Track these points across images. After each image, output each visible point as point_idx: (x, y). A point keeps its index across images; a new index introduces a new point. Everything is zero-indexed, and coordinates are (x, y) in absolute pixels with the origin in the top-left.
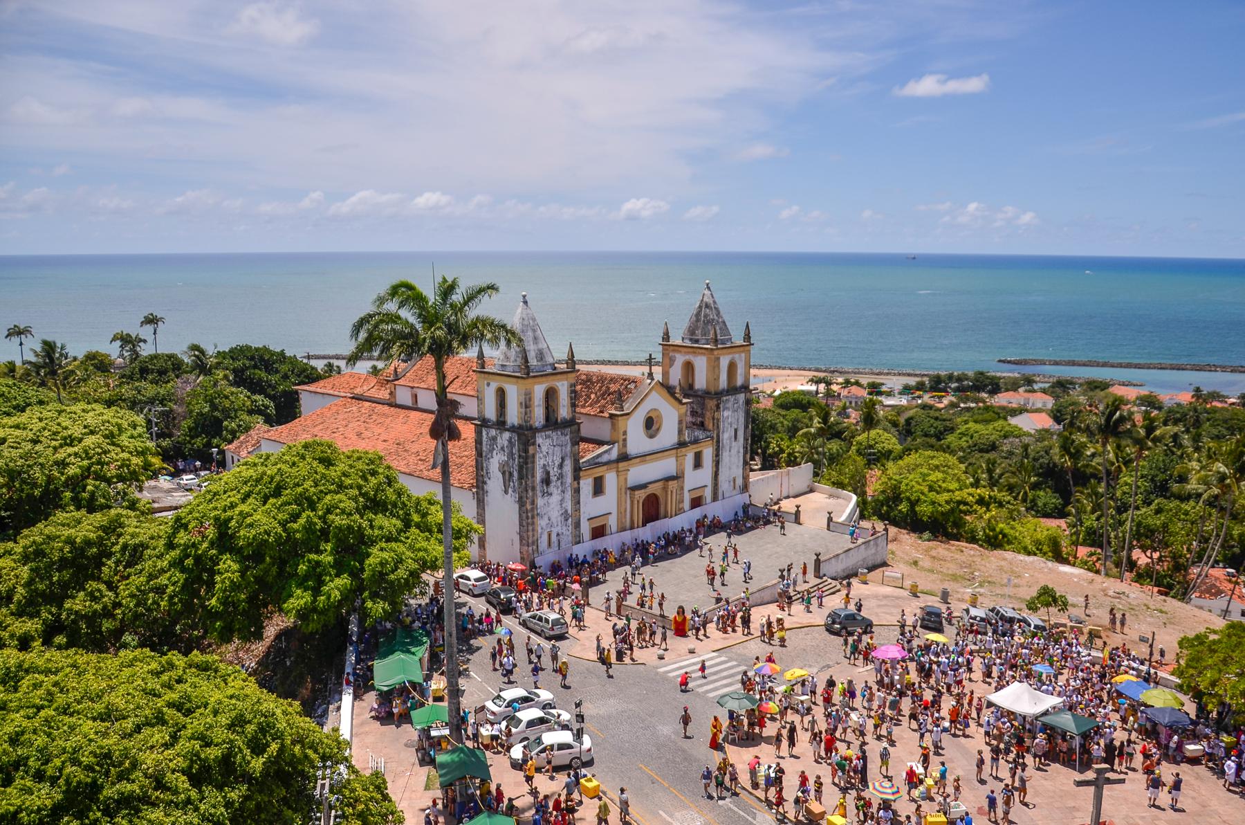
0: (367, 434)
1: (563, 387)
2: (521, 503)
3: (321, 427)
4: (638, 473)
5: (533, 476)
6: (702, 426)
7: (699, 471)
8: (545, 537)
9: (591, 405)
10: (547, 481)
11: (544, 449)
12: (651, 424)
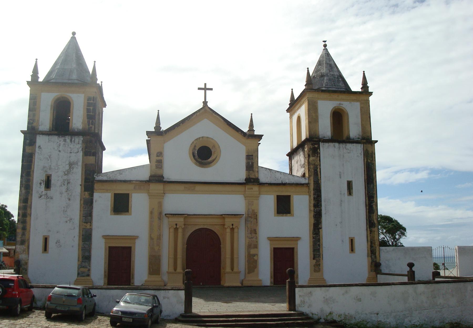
4: (177, 202)
10: (48, 184)
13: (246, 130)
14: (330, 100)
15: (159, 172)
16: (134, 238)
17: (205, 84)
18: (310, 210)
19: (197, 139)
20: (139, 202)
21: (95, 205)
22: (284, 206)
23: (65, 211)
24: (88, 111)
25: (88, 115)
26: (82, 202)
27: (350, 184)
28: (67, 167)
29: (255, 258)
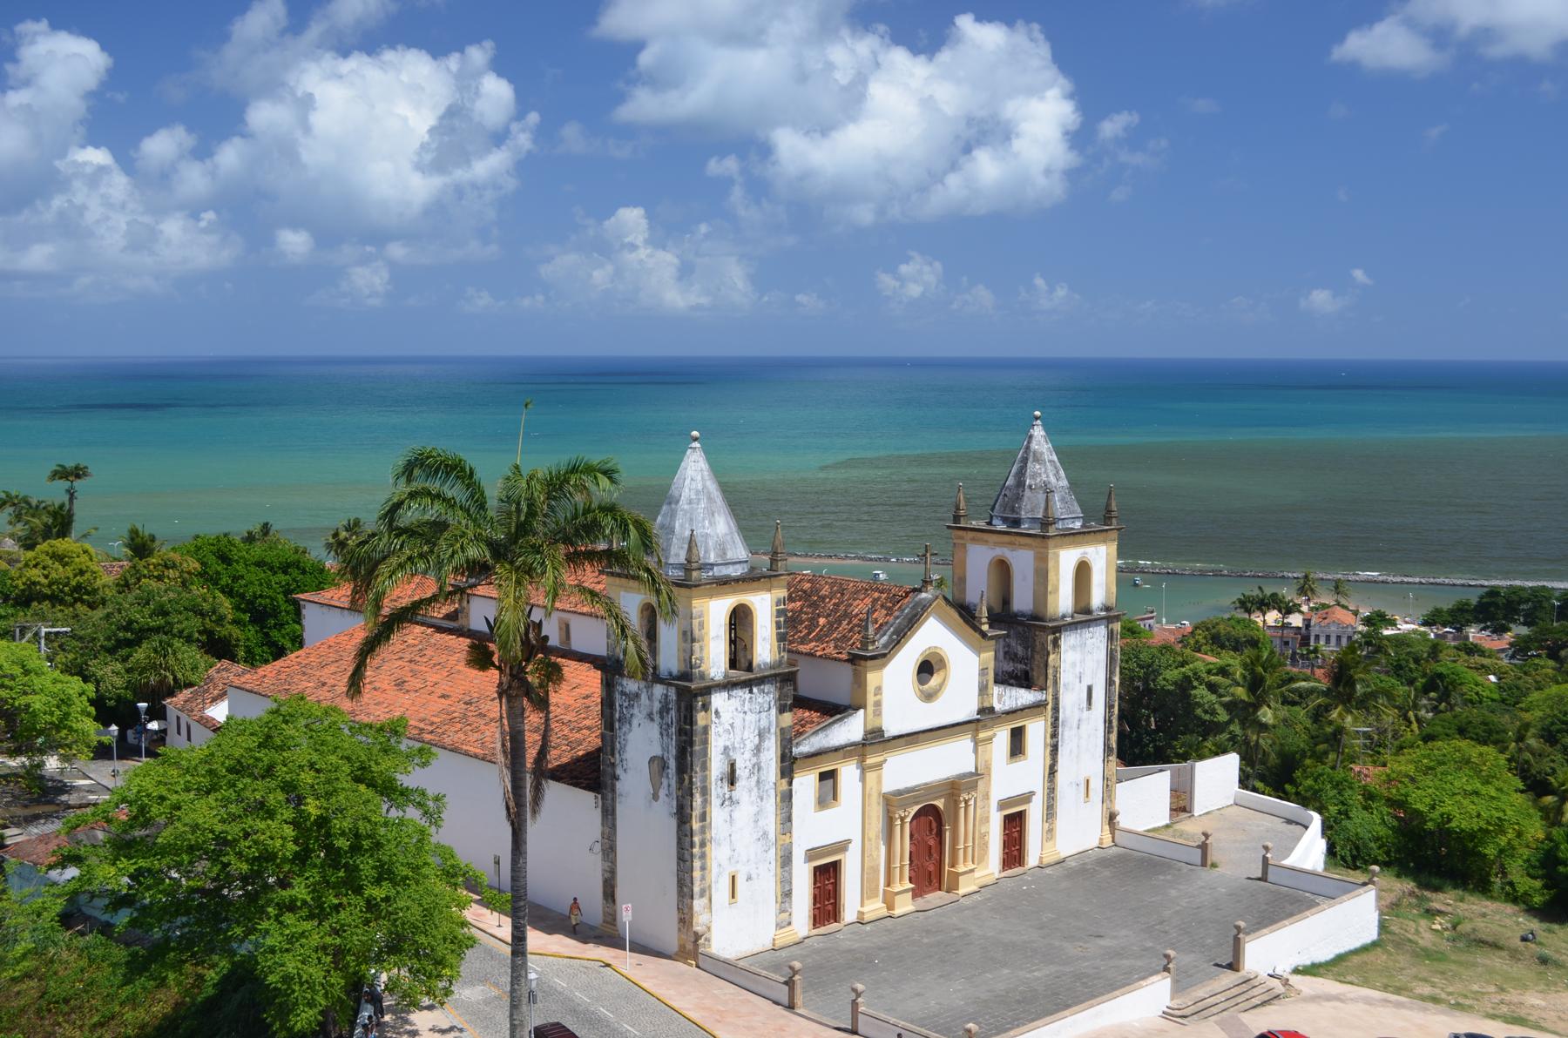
0: (415, 683)
1: (764, 605)
2: (683, 816)
3: (333, 668)
5: (705, 767)
6: (1024, 680)
7: (1020, 765)
8: (727, 882)
9: (819, 639)
11: (726, 717)
23: (756, 821)
27: (1090, 689)
28: (757, 740)
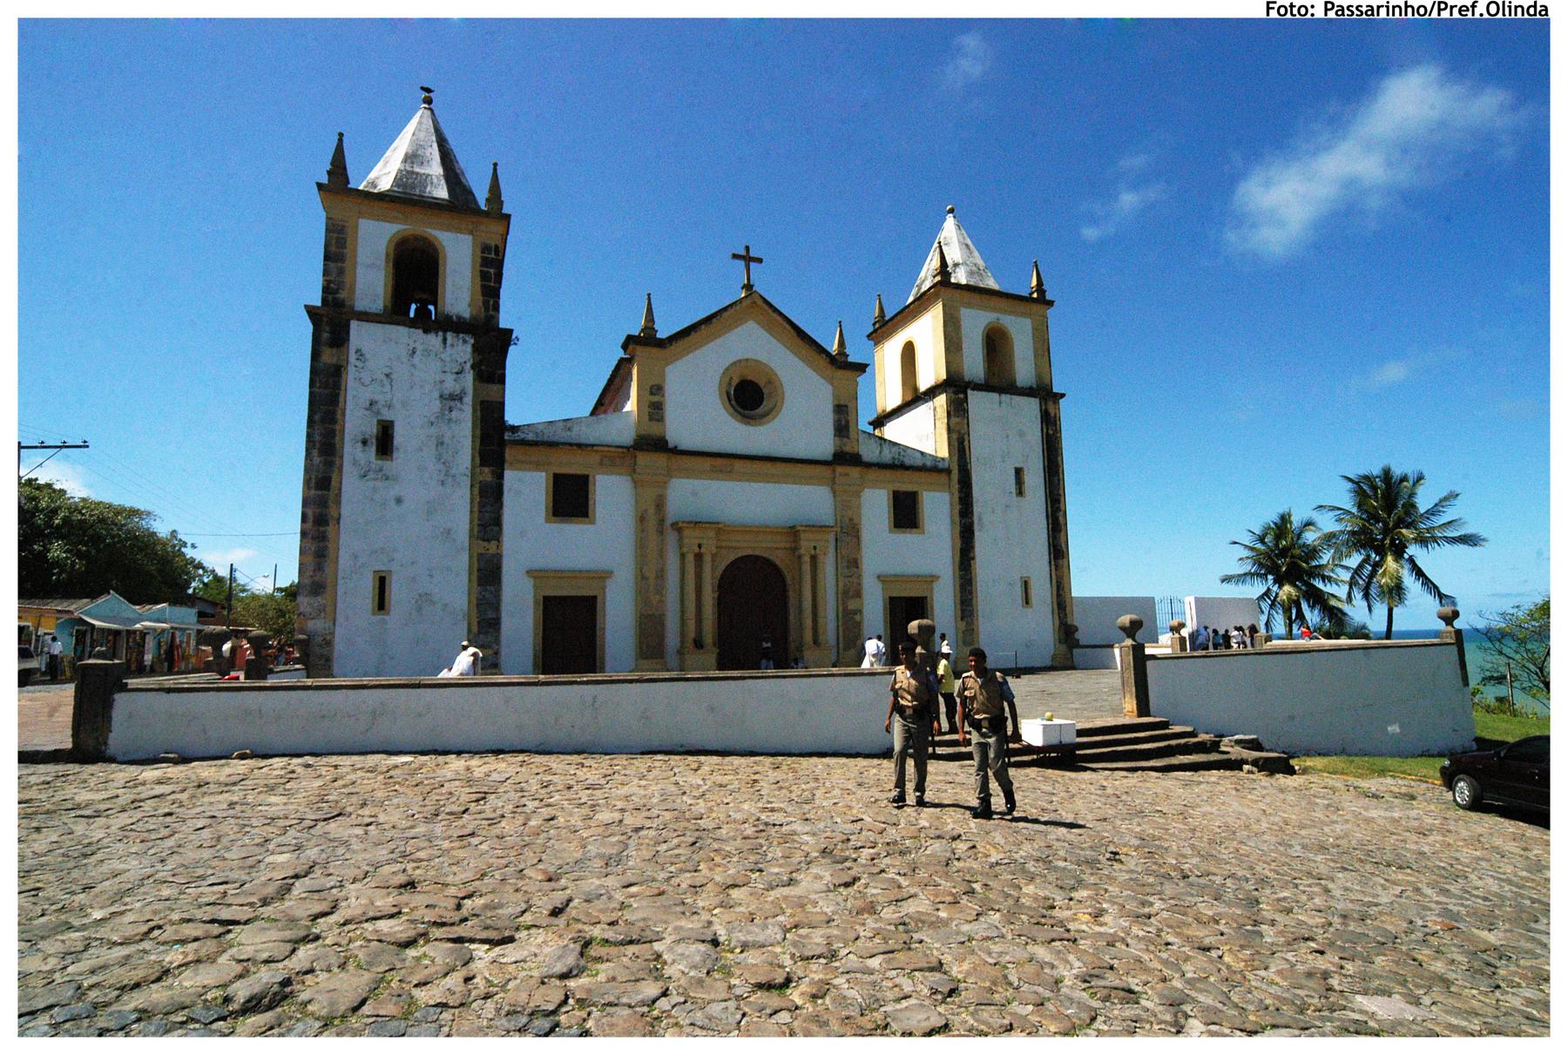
10: (384, 442)
12: (749, 396)
13: (834, 348)
14: (980, 307)
15: (653, 429)
16: (603, 576)
17: (747, 248)
18: (953, 522)
19: (734, 364)
20: (612, 494)
21: (508, 498)
22: (906, 514)
24: (484, 276)
25: (483, 287)
26: (476, 491)
29: (857, 617)
